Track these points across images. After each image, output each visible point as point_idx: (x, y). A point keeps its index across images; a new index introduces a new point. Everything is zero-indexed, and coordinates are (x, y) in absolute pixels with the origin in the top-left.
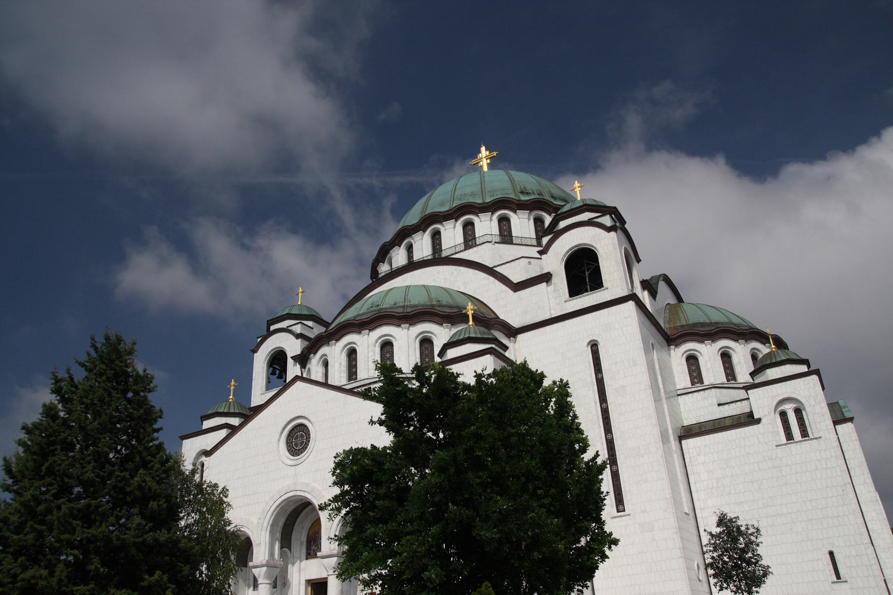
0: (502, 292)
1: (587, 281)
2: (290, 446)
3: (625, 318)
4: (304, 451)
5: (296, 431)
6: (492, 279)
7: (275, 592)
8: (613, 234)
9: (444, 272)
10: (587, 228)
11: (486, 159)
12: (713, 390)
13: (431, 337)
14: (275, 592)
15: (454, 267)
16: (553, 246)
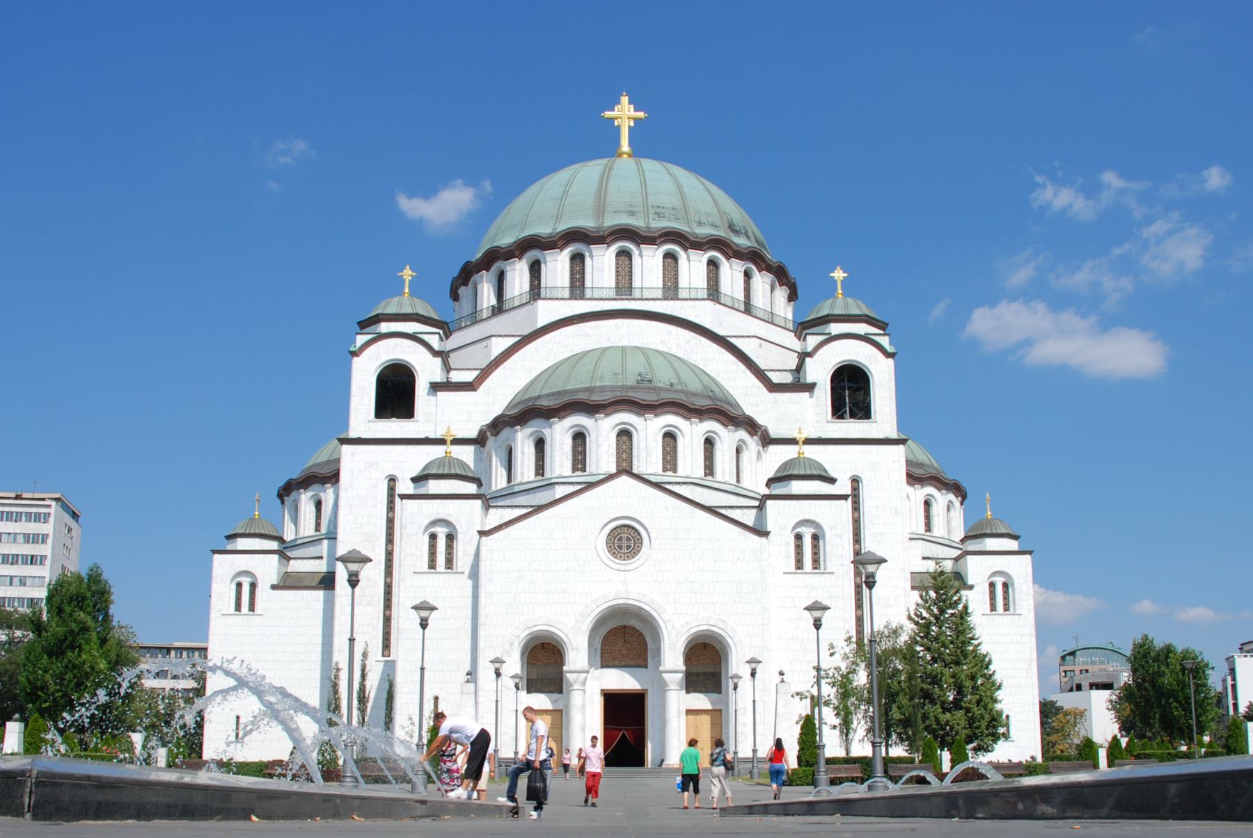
0: (754, 386)
1: (847, 401)
2: (610, 547)
3: (894, 461)
4: (633, 557)
5: (620, 532)
6: (742, 366)
7: (560, 698)
8: (891, 361)
9: (677, 335)
10: (863, 343)
11: (629, 118)
12: (920, 541)
13: (714, 438)
14: (560, 698)
15: (692, 334)
16: (821, 351)
